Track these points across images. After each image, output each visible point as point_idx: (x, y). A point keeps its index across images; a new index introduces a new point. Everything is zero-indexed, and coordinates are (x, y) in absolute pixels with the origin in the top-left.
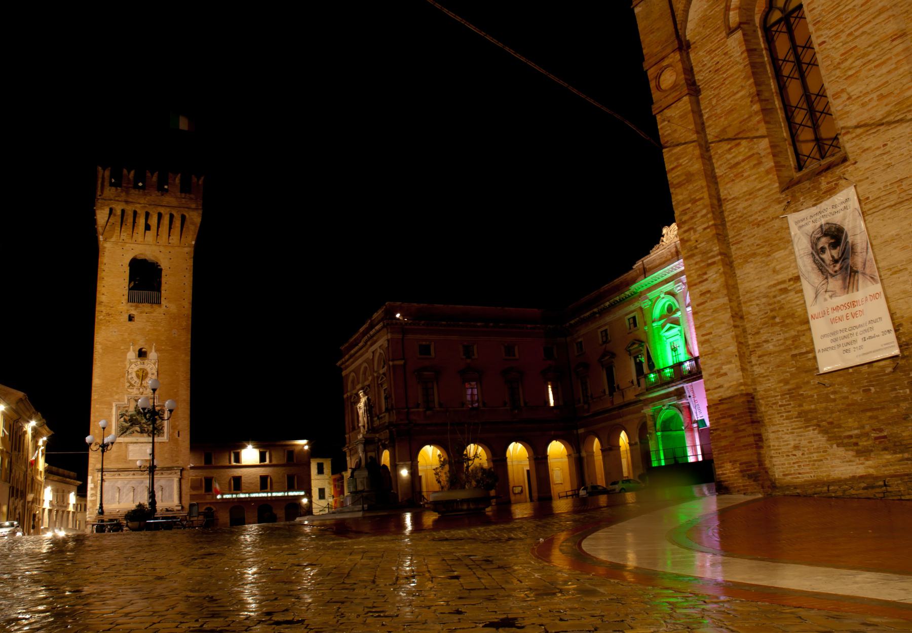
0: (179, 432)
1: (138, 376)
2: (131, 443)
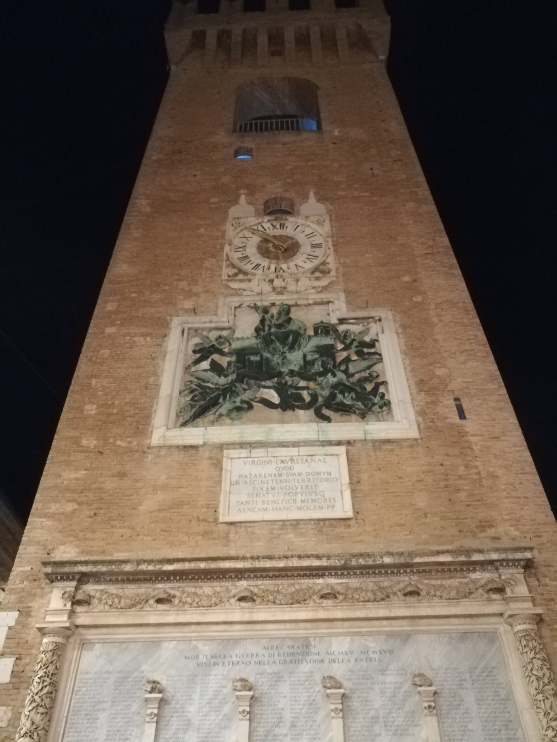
2: (242, 445)
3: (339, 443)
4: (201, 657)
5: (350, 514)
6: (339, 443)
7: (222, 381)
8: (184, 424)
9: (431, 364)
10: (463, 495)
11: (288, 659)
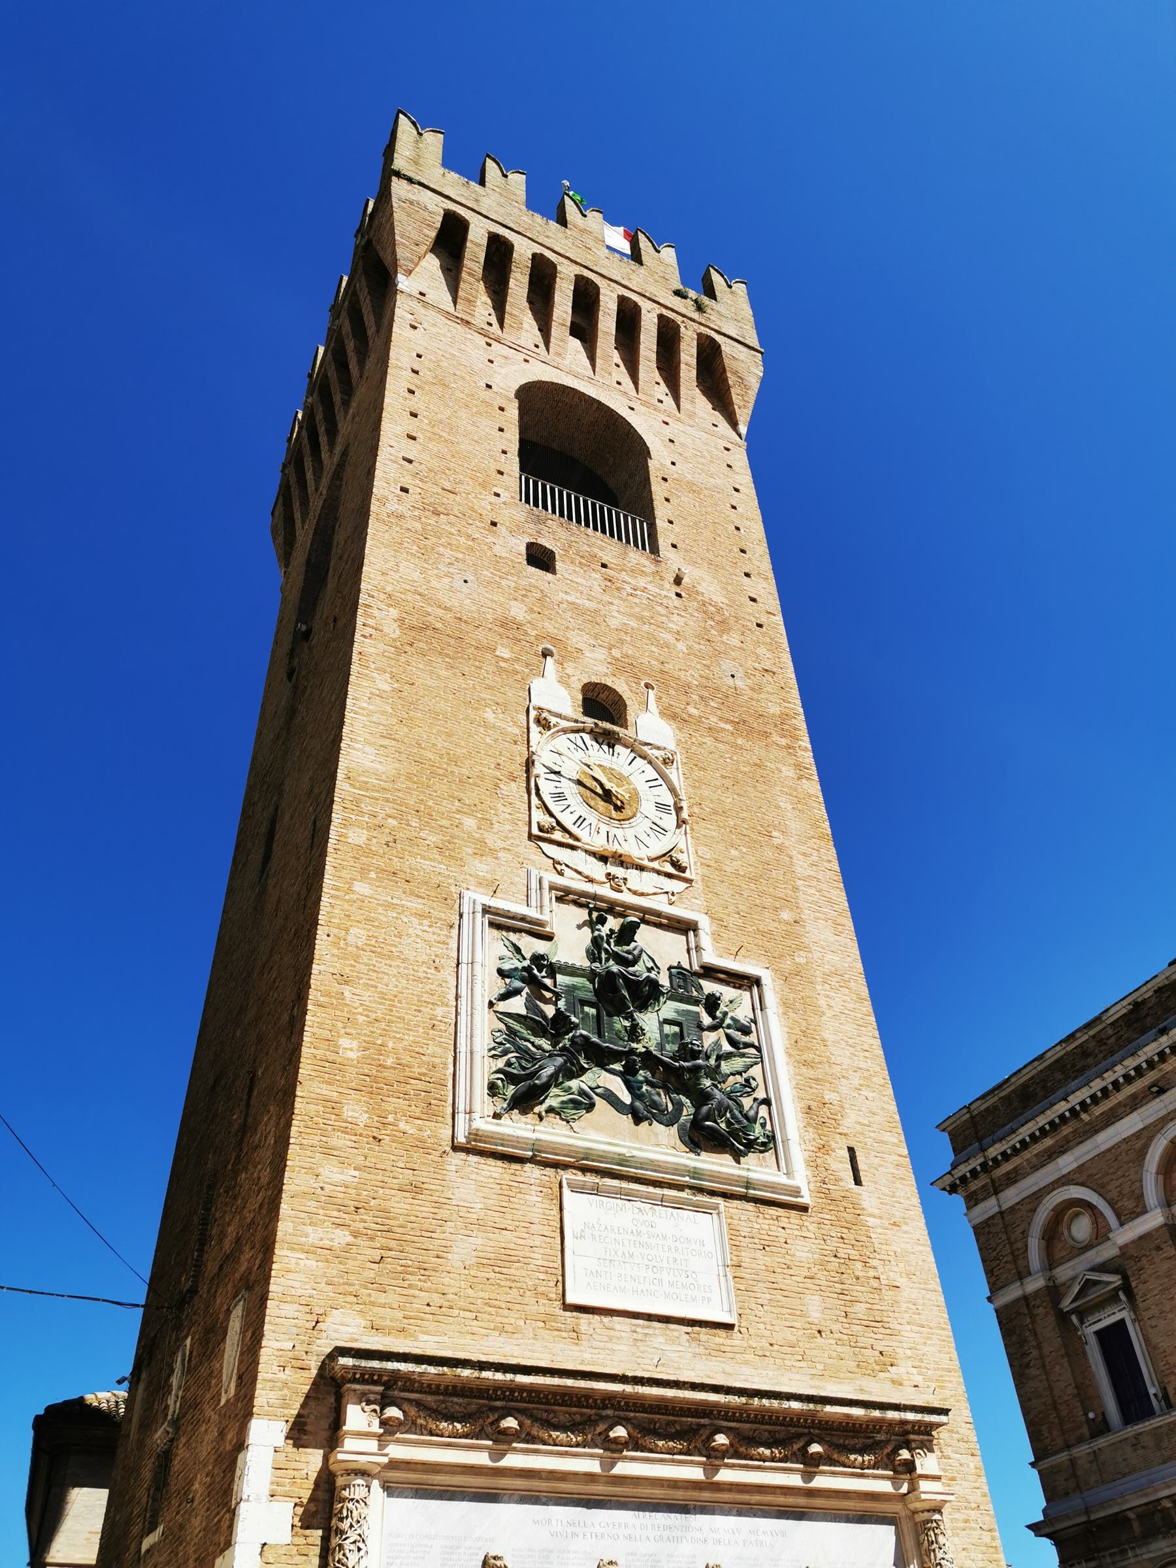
0: (851, 1150)
4: (554, 1522)
10: (860, 1309)
11: (665, 1534)
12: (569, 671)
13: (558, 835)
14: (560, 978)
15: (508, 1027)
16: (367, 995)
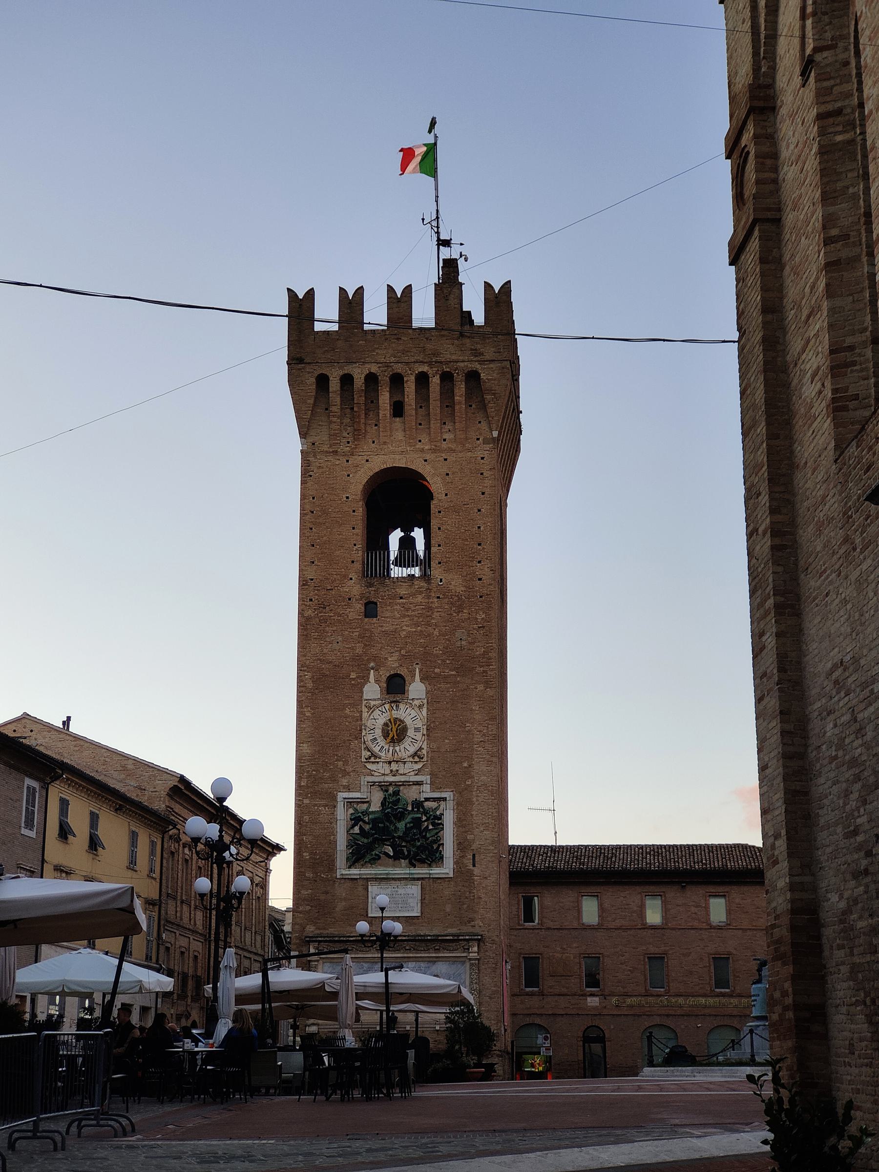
0: (474, 856)
1: (386, 734)
3: (418, 879)
5: (419, 915)
6: (418, 879)
7: (366, 841)
8: (350, 867)
9: (466, 832)
10: (465, 906)
12: (381, 673)
13: (372, 760)
14: (370, 817)
15: (354, 838)
16: (310, 838)
